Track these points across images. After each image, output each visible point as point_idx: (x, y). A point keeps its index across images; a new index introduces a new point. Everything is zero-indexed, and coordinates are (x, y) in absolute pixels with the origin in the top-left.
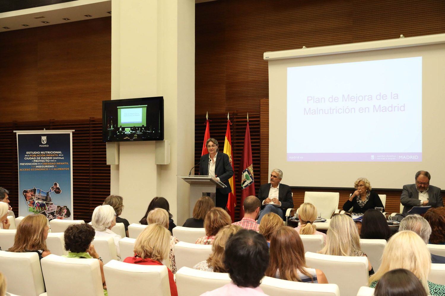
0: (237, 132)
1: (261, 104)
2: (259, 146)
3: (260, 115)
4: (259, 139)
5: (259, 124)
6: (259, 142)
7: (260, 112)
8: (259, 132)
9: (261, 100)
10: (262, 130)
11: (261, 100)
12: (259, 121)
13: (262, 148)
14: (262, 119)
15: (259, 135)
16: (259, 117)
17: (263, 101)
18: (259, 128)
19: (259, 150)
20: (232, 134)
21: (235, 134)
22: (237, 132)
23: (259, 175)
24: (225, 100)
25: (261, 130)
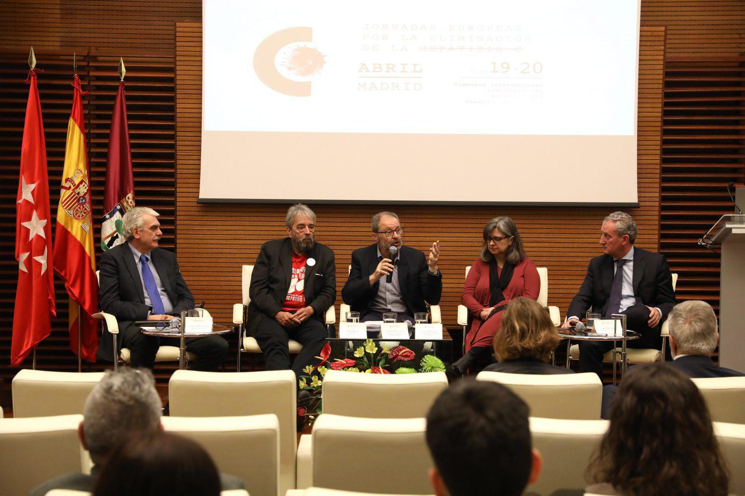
1: (178, 34)
2: (173, 147)
3: (175, 63)
4: (173, 128)
5: (173, 90)
6: (173, 137)
7: (175, 58)
8: (173, 109)
9: (178, 24)
10: (182, 106)
11: (178, 24)
12: (172, 80)
13: (181, 150)
14: (182, 77)
15: (173, 118)
16: (173, 70)
17: (183, 26)
18: (173, 99)
19: (173, 156)
20: (86, 112)
21: (92, 112)
22: (99, 107)
23: (173, 222)
24: (58, 16)
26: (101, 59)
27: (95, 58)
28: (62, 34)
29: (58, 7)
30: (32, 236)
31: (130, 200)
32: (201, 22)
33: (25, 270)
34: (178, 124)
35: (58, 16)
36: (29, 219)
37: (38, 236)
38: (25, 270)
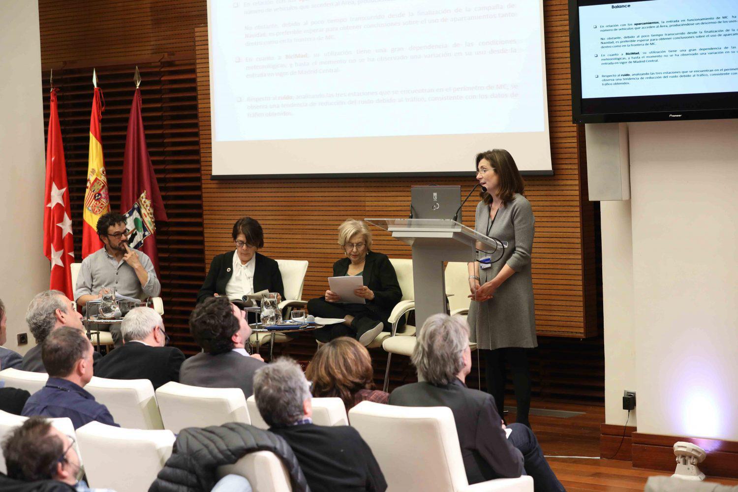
0: (173, 109)
11: (196, 29)
12: (194, 80)
19: (197, 152)
25: (200, 106)
26: (177, 63)
27: (170, 64)
28: (152, 43)
29: (150, 18)
30: (65, 234)
31: (144, 200)
32: (207, 26)
33: (60, 263)
34: (201, 124)
35: (150, 27)
36: (61, 220)
37: (69, 233)
38: (60, 263)
